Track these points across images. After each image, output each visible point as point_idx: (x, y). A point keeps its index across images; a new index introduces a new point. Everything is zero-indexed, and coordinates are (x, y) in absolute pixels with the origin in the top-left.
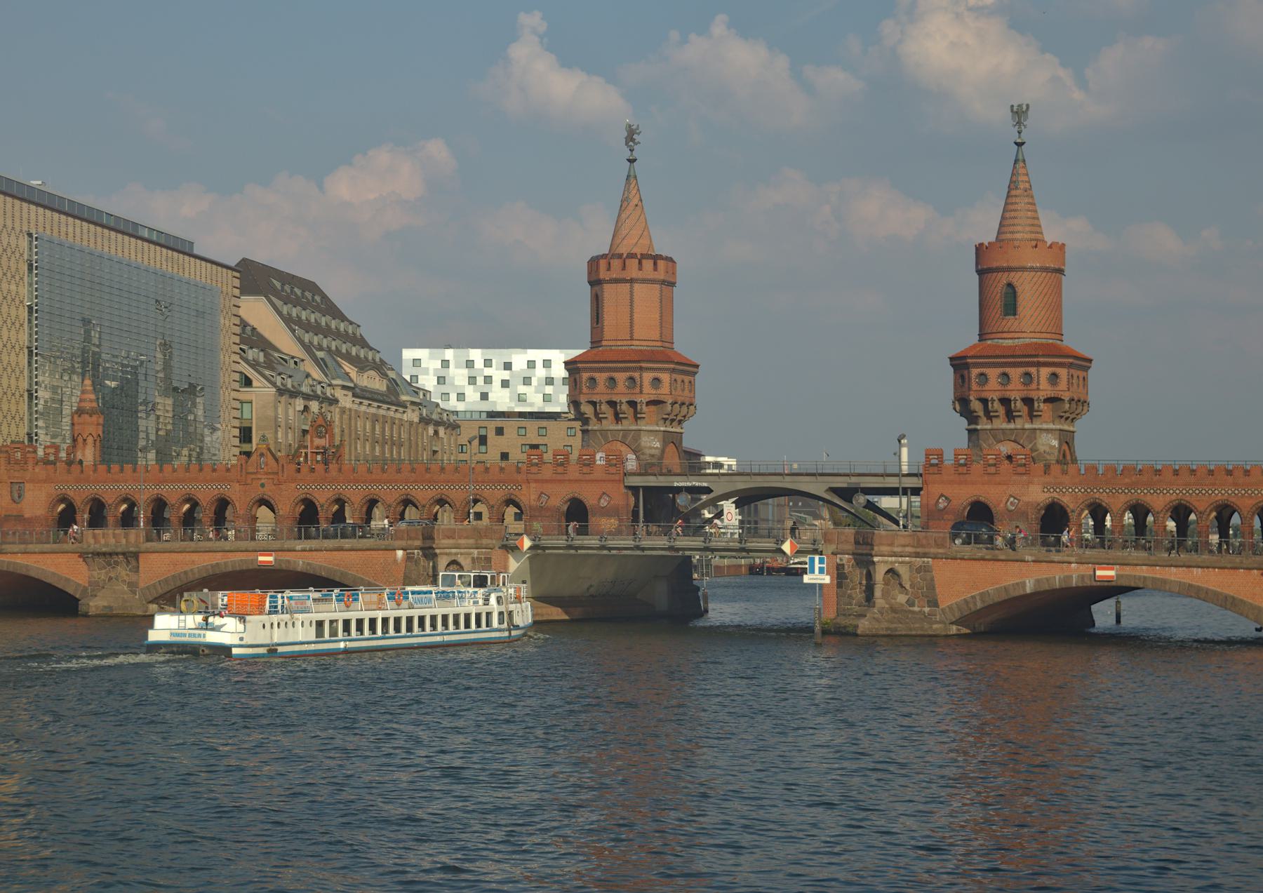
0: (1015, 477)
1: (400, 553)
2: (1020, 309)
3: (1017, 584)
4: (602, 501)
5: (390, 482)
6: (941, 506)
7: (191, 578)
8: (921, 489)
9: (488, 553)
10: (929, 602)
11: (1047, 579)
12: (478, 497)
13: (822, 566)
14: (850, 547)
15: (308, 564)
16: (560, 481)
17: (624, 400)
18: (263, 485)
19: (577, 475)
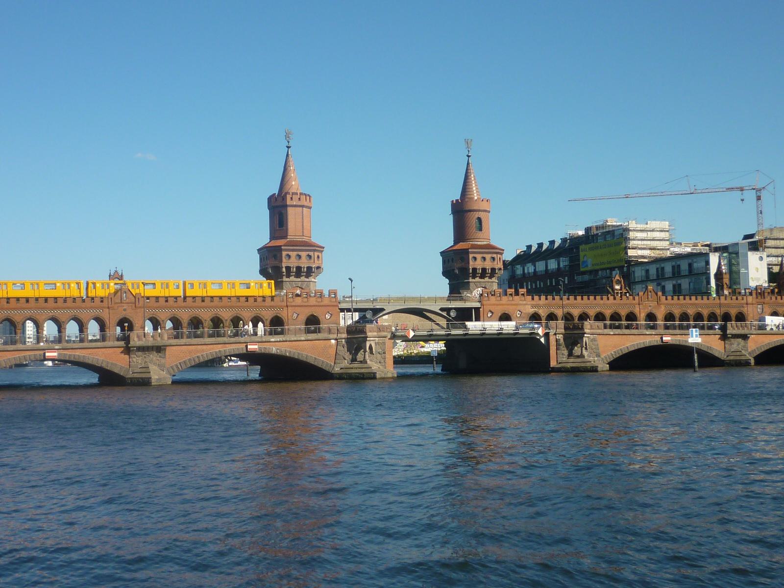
0: (521, 302)
1: (333, 341)
2: (483, 229)
3: (632, 345)
4: (327, 316)
5: (206, 307)
6: (489, 315)
7: (202, 360)
8: (480, 308)
9: (384, 340)
10: (596, 355)
11: (643, 343)
12: (258, 315)
13: (696, 333)
14: (563, 331)
15: (277, 349)
16: (305, 306)
17: (306, 266)
18: (125, 310)
19: (315, 303)
